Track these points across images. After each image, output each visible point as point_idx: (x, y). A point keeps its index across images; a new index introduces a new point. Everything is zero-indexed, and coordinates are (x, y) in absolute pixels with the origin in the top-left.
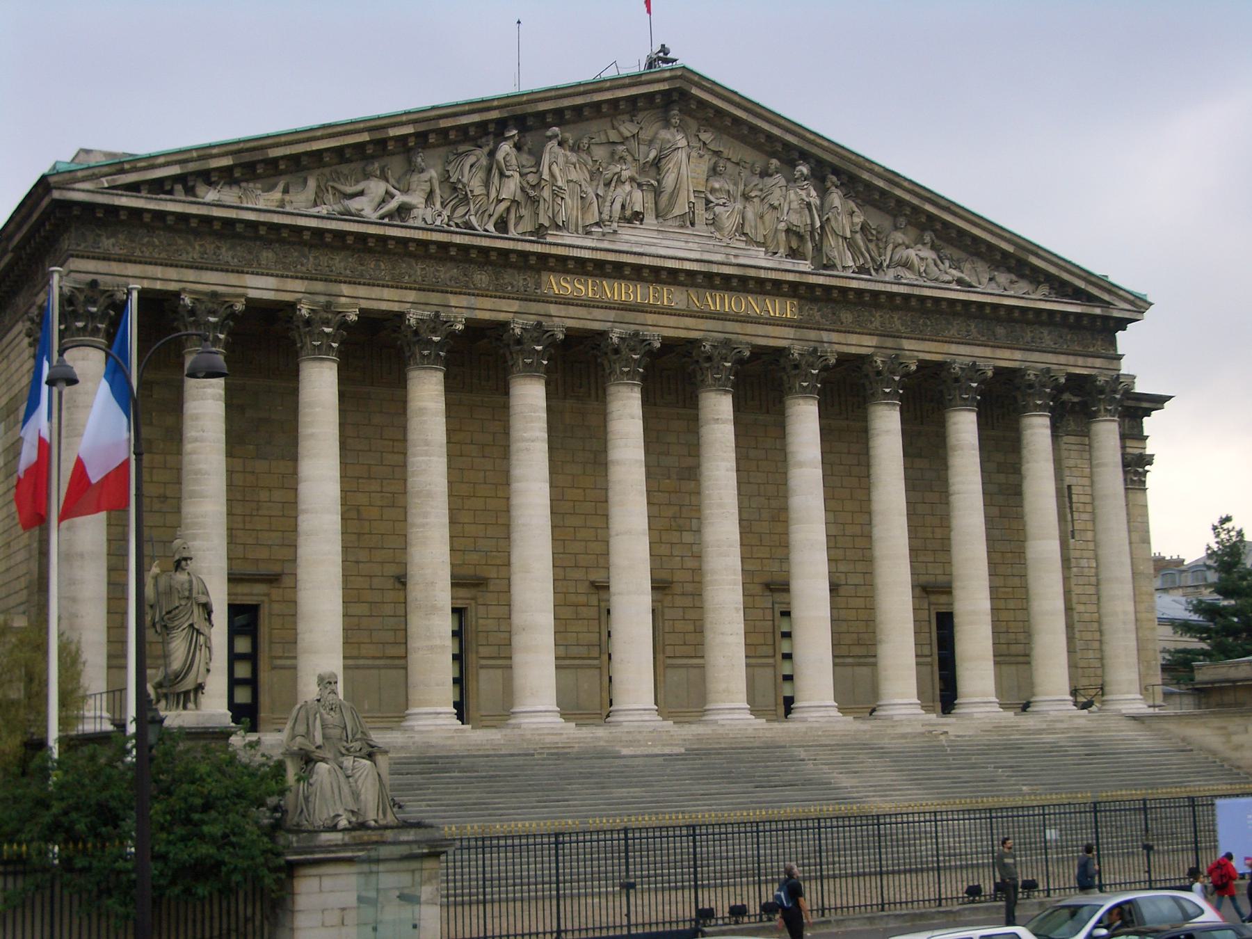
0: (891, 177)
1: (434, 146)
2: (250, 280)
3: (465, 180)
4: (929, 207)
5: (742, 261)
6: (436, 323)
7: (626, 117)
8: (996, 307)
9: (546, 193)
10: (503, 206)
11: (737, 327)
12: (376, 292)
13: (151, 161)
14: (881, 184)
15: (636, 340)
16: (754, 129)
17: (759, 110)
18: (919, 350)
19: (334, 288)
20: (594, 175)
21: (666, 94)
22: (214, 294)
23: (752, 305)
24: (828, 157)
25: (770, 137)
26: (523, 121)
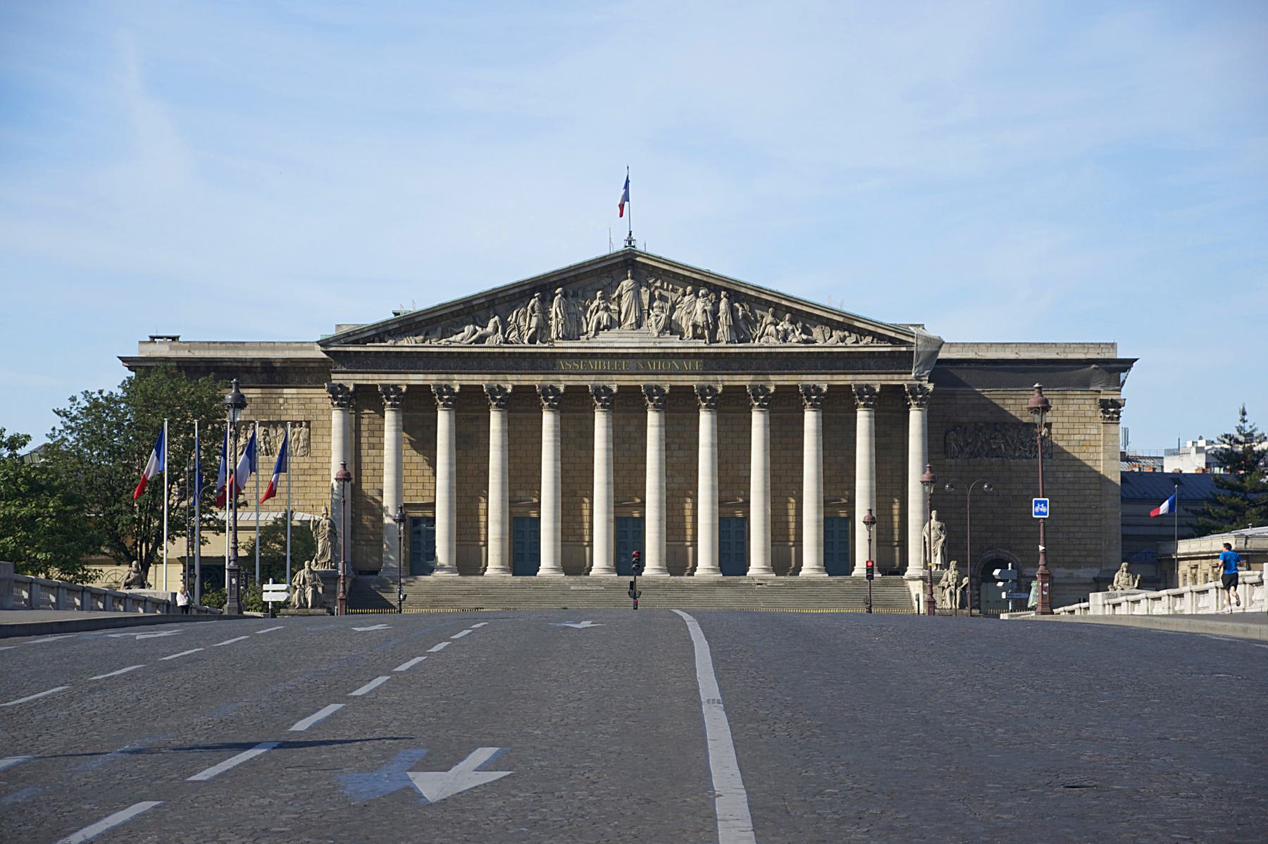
2: (411, 376)
4: (784, 302)
11: (665, 377)
12: (471, 377)
13: (362, 331)
14: (753, 293)
18: (775, 381)
19: (451, 377)
21: (625, 261)
22: (394, 386)
26: (542, 287)
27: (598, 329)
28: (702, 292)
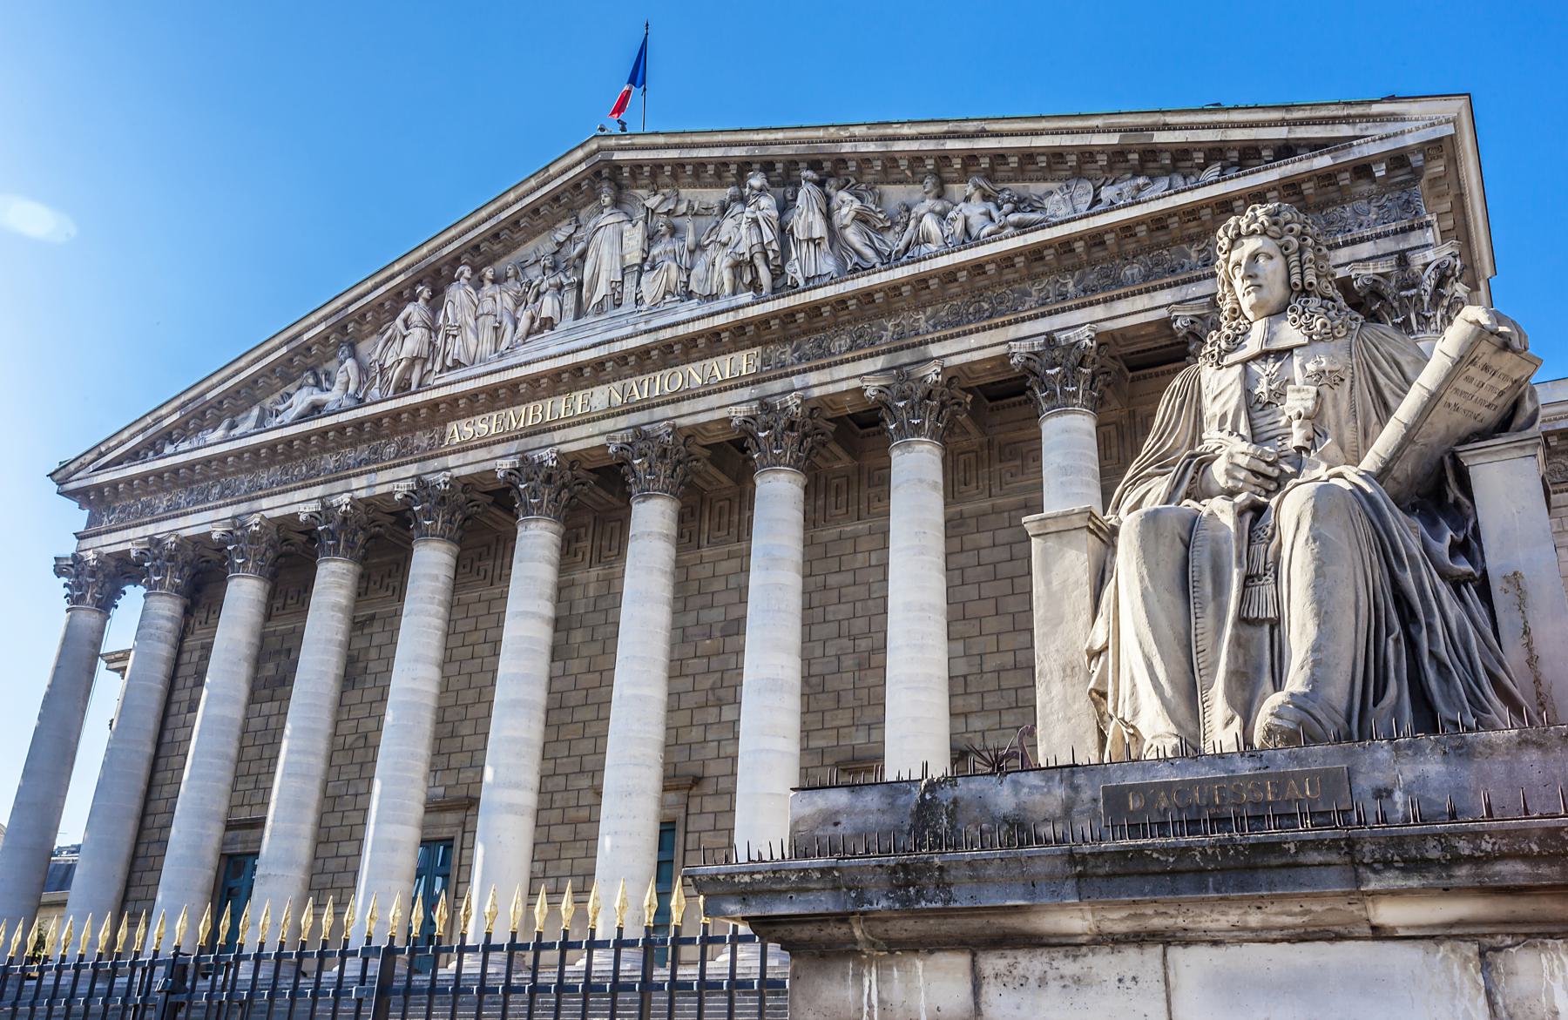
4: (951, 145)
5: (653, 325)
6: (327, 510)
8: (1095, 239)
11: (669, 411)
14: (872, 147)
15: (527, 467)
16: (700, 165)
19: (256, 505)
20: (519, 301)
21: (596, 174)
23: (694, 373)
24: (790, 150)
27: (529, 334)
28: (757, 181)
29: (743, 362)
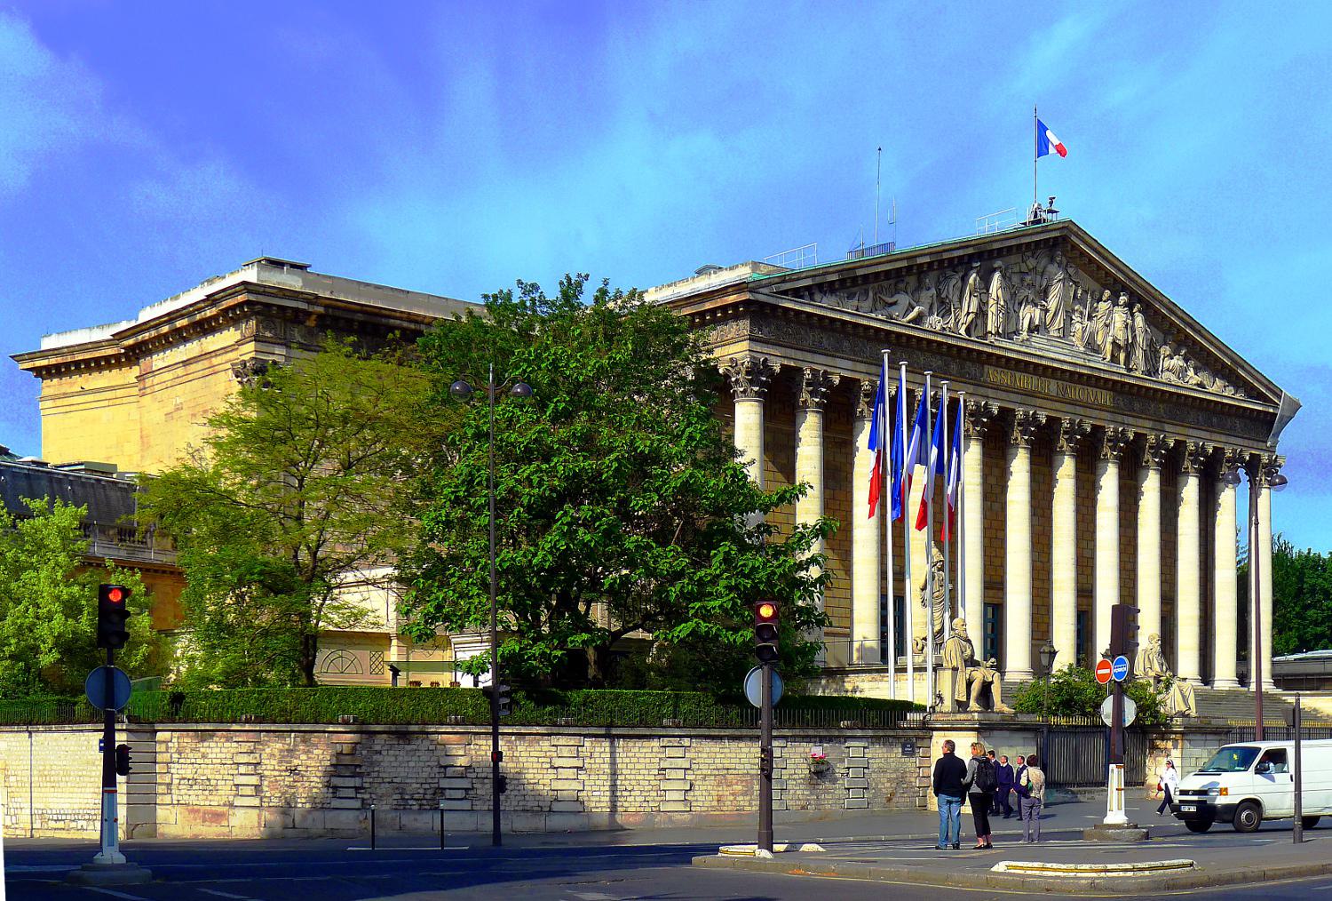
0: (1172, 307)
1: (935, 270)
3: (950, 297)
5: (1092, 364)
7: (1029, 254)
9: (993, 309)
10: (971, 317)
13: (798, 276)
16: (1100, 267)
17: (1106, 255)
25: (1108, 273)
28: (1123, 299)
29: (1105, 397)
